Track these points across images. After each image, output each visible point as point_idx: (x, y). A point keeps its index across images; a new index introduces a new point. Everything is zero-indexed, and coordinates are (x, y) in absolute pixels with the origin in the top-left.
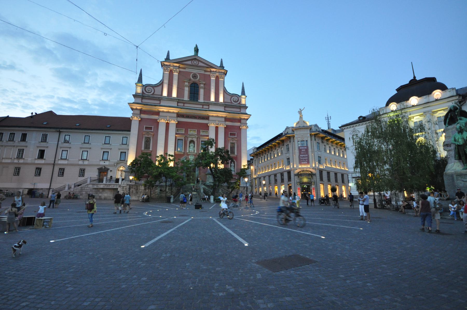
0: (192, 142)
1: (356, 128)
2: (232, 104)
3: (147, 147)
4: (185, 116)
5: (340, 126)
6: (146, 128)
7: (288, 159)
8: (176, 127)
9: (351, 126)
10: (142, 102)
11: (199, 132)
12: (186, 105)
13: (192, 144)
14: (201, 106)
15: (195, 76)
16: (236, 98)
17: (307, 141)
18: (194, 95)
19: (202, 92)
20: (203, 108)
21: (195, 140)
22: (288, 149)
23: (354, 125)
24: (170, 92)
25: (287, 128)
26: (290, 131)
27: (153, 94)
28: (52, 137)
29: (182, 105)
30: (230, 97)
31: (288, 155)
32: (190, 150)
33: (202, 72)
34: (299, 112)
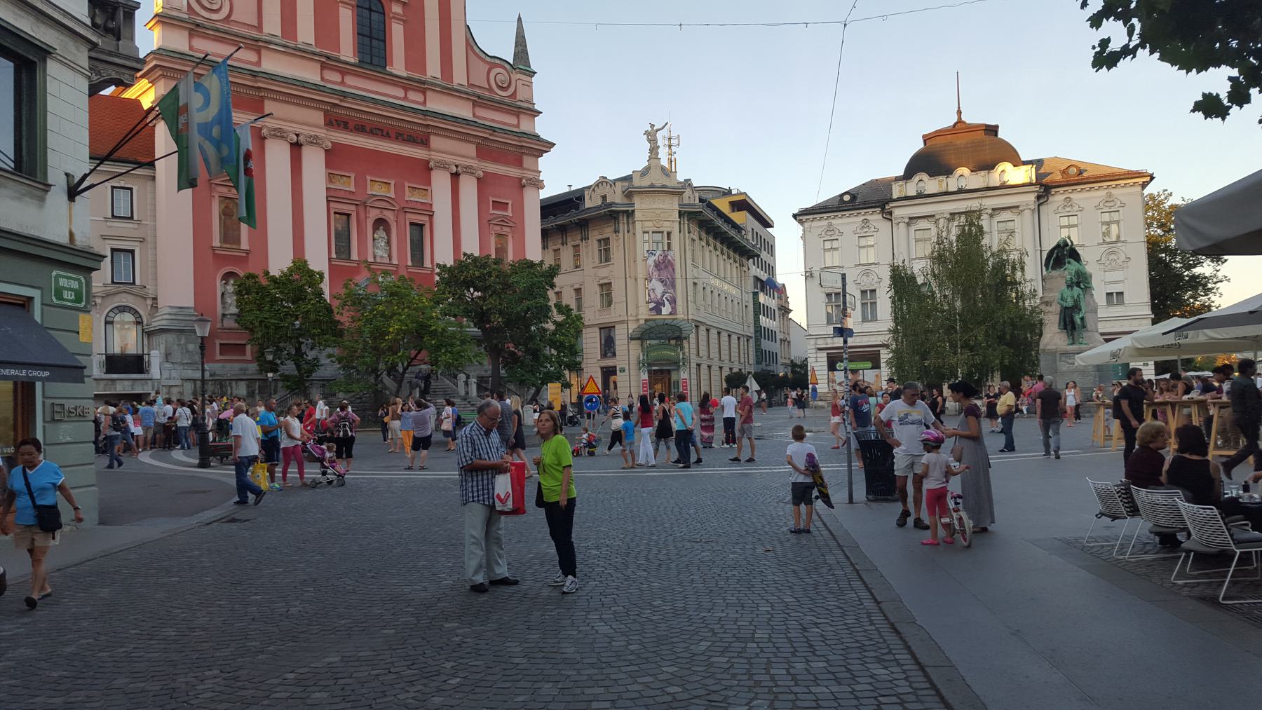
0: (380, 223)
1: (834, 222)
2: (494, 96)
4: (351, 125)
5: (796, 212)
7: (606, 287)
8: (327, 166)
9: (825, 215)
10: (191, 48)
11: (399, 189)
12: (350, 80)
13: (381, 233)
14: (400, 93)
16: (500, 75)
17: (669, 234)
19: (397, 32)
20: (405, 98)
21: (389, 216)
22: (605, 256)
23: (832, 215)
25: (603, 181)
26: (616, 197)
27: (227, 19)
29: (336, 77)
30: (487, 67)
31: (604, 272)
32: (379, 253)
34: (647, 133)
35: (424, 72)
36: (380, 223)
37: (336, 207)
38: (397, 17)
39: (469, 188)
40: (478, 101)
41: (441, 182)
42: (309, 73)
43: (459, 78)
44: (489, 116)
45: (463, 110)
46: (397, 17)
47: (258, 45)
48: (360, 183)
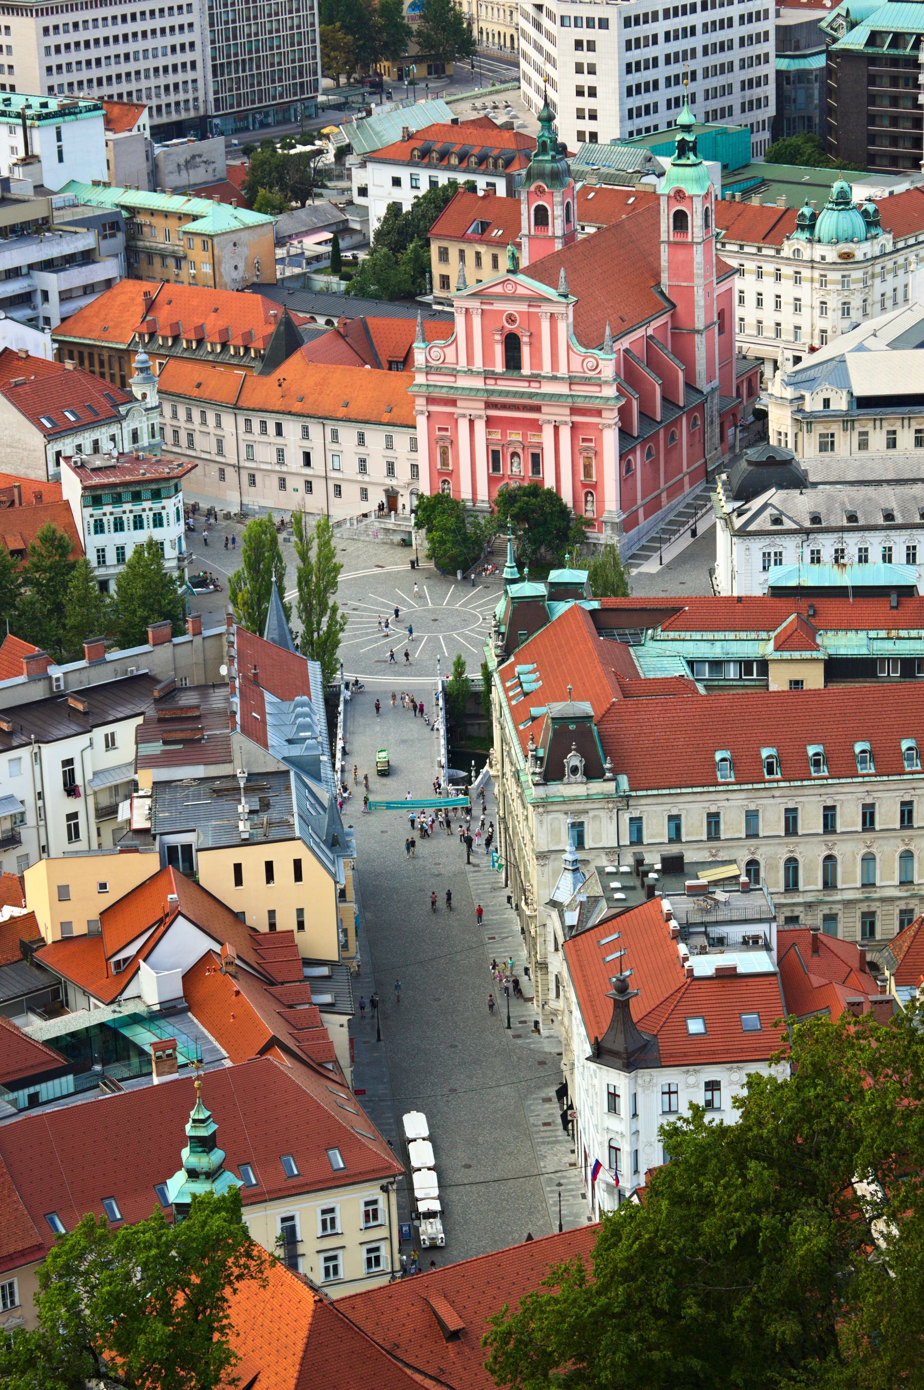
0: (514, 454)
3: (445, 462)
6: (440, 429)
8: (487, 427)
11: (524, 435)
12: (499, 382)
13: (516, 459)
14: (526, 384)
15: (511, 319)
18: (513, 361)
19: (526, 351)
21: (520, 451)
24: (470, 359)
27: (443, 362)
28: (315, 430)
29: (493, 382)
33: (523, 308)
35: (541, 369)
36: (514, 454)
37: (491, 448)
38: (526, 343)
39: (565, 433)
40: (572, 381)
41: (548, 431)
42: (478, 383)
43: (563, 371)
44: (580, 390)
45: (562, 389)
46: (526, 343)
47: (454, 373)
48: (504, 434)
